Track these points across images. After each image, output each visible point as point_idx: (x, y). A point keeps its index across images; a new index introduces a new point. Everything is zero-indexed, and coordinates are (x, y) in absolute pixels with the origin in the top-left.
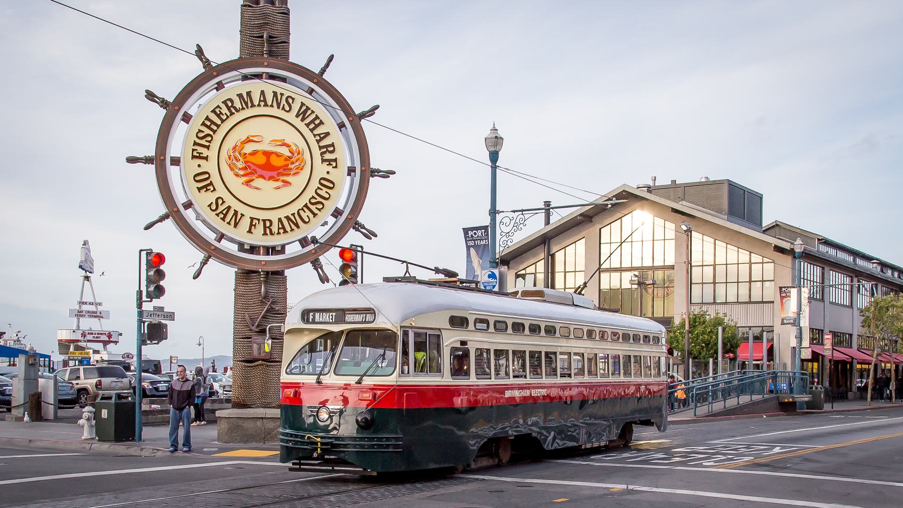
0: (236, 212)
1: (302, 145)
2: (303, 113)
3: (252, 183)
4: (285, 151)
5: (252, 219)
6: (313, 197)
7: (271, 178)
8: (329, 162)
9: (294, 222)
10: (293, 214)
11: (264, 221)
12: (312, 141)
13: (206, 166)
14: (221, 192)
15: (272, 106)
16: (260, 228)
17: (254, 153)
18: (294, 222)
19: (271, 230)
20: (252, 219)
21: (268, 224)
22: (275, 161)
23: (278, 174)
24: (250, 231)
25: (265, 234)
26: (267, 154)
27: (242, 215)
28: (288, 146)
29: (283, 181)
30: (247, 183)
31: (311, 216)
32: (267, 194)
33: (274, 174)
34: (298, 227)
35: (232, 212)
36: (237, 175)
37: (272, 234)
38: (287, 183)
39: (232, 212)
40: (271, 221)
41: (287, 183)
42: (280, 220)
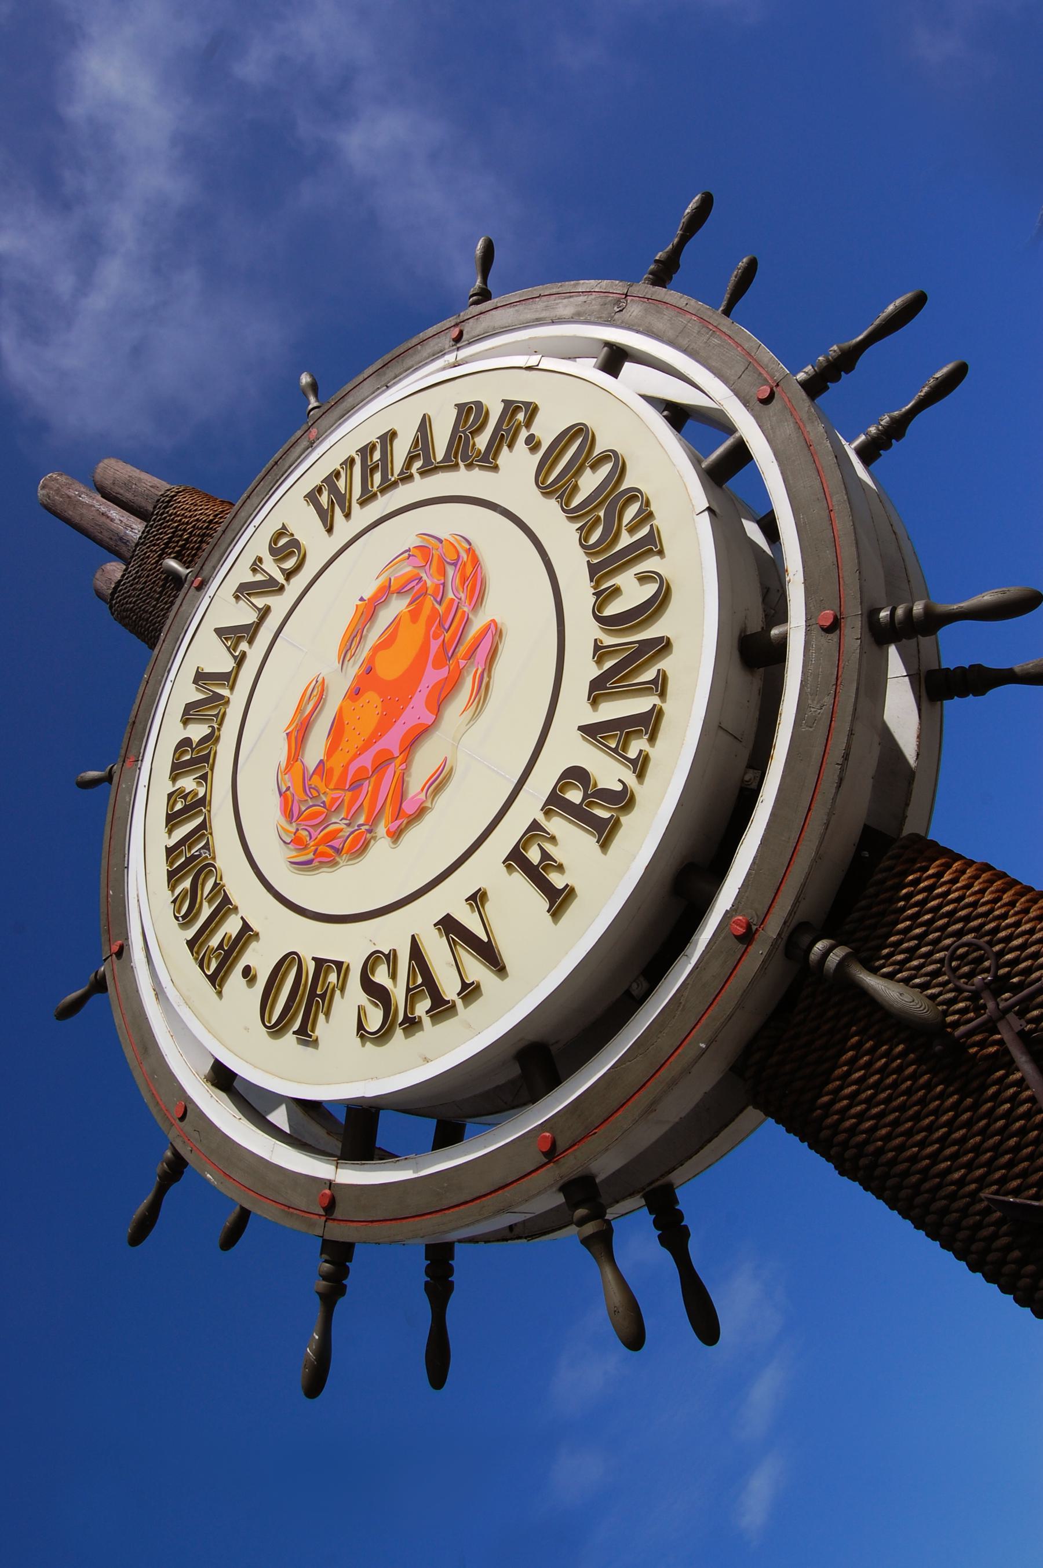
0: (449, 925)
1: (403, 534)
2: (330, 502)
5: (516, 859)
6: (585, 533)
7: (439, 702)
8: (504, 438)
9: (631, 659)
10: (600, 652)
11: (555, 802)
13: (261, 958)
15: (265, 613)
16: (571, 842)
18: (631, 659)
19: (607, 796)
20: (516, 859)
21: (575, 796)
24: (559, 900)
25: (606, 833)
27: (477, 899)
29: (471, 654)
32: (488, 753)
34: (663, 646)
35: (438, 952)
37: (623, 800)
39: (438, 952)
40: (576, 775)
42: (590, 731)
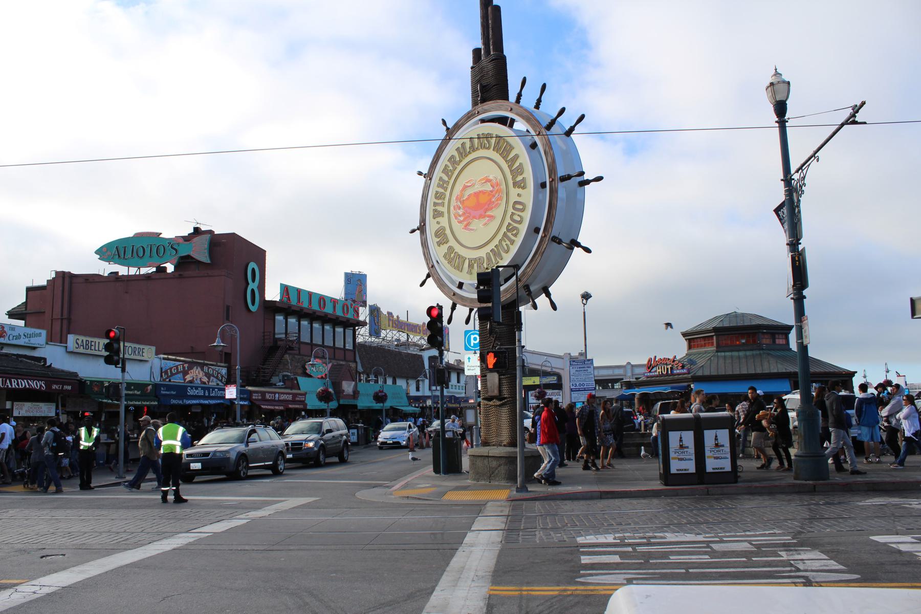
3: (471, 227)
4: (488, 187)
7: (482, 216)
12: (505, 166)
14: (452, 242)
17: (470, 196)
22: (483, 199)
23: (486, 210)
26: (477, 194)
28: (488, 181)
30: (466, 227)
31: (508, 243)
33: (481, 212)
36: (460, 222)
38: (492, 217)
41: (492, 217)
